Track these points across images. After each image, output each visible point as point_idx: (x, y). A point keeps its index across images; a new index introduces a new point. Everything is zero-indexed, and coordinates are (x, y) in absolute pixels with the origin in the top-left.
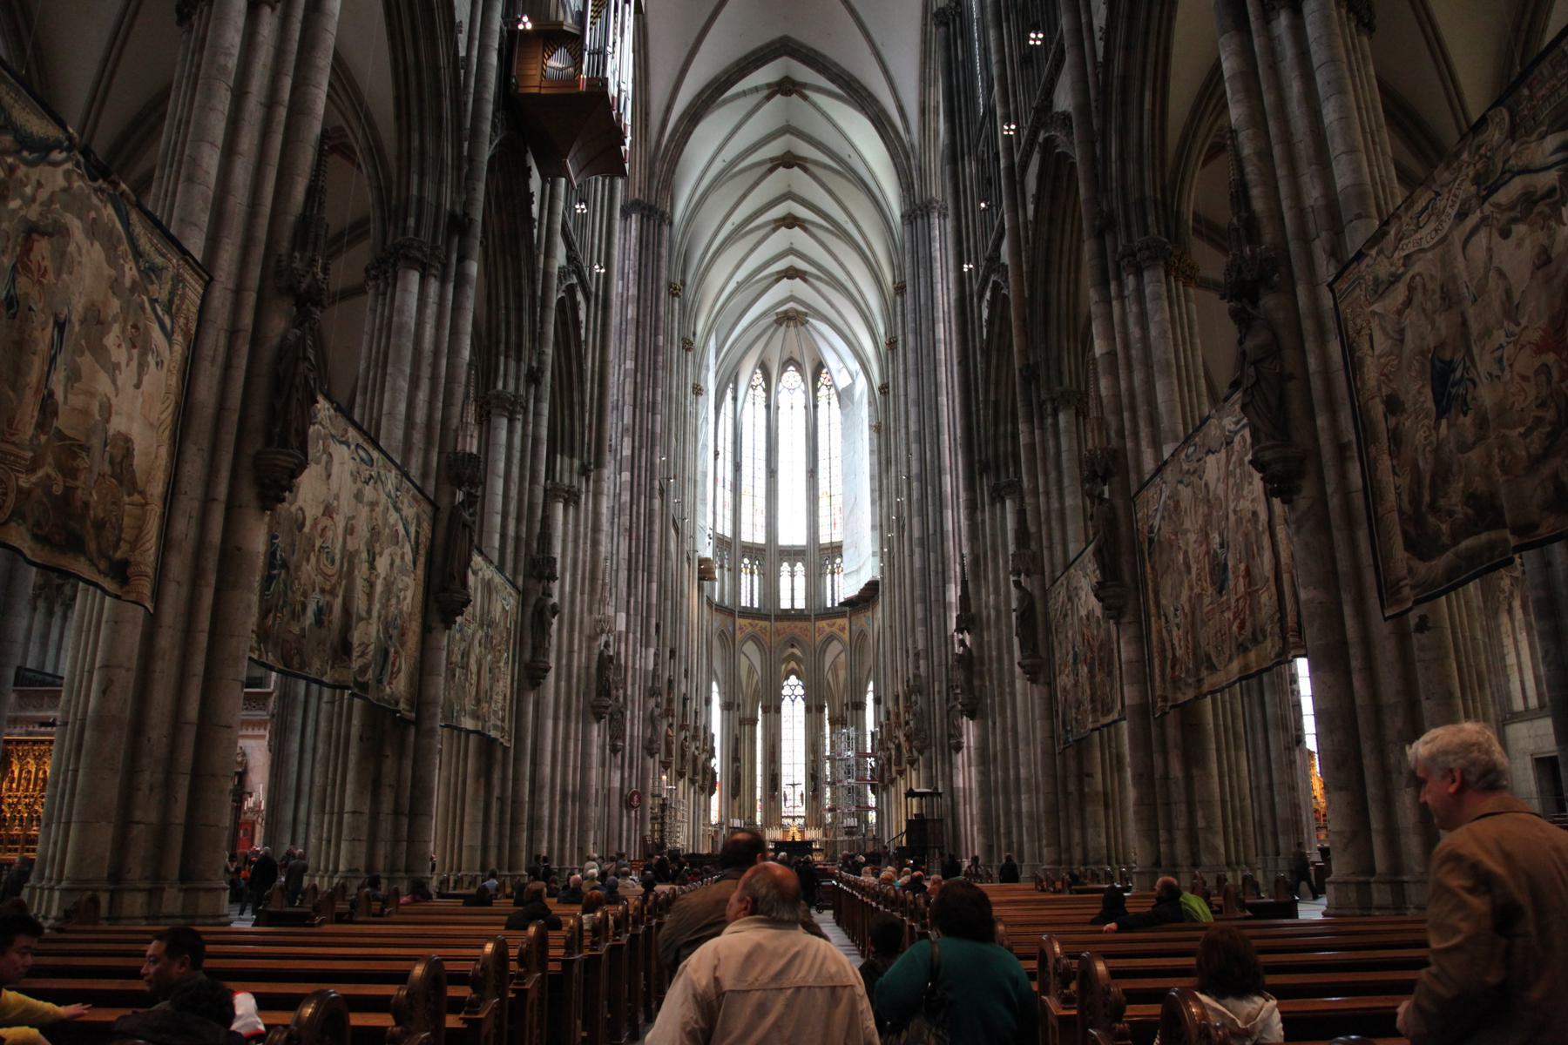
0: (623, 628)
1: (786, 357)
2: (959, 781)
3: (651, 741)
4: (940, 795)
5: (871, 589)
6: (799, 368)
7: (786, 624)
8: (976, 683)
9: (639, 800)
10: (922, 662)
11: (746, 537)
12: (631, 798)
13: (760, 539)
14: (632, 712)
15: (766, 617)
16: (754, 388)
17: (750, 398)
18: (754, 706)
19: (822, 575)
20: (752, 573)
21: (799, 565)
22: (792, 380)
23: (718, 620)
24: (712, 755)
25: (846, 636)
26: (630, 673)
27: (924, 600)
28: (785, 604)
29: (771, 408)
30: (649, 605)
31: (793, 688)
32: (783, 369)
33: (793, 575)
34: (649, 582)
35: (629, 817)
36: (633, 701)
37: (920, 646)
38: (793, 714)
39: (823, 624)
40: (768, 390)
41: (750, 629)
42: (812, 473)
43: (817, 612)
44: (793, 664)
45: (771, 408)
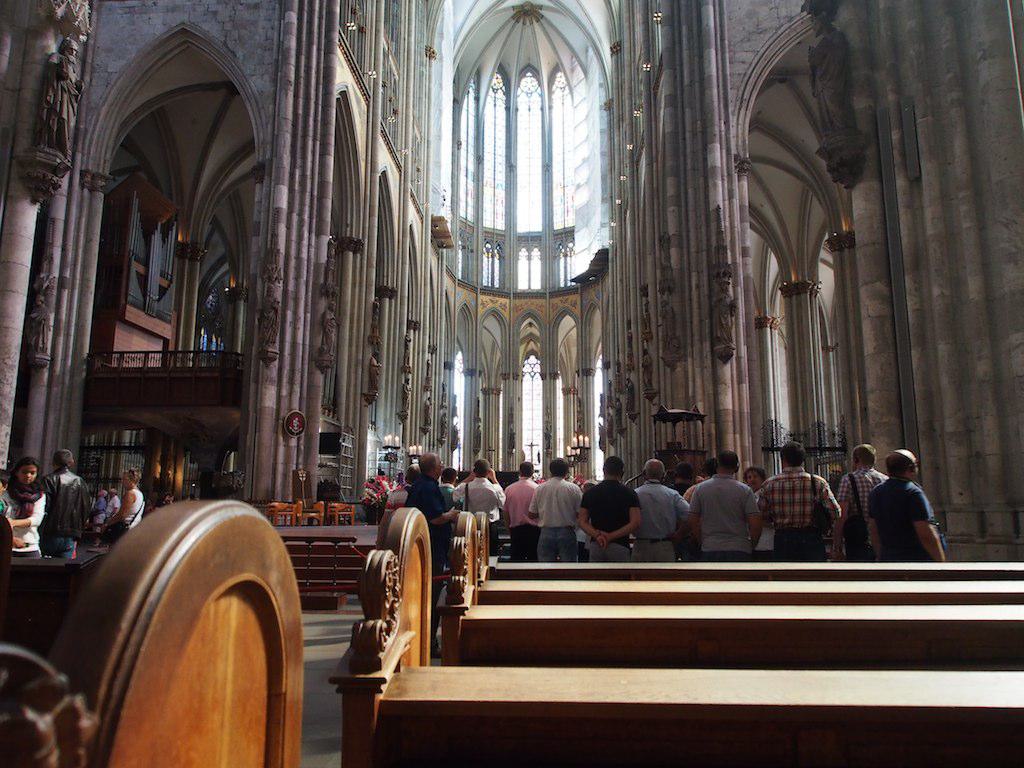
0: (284, 204)
1: (523, 64)
2: (728, 402)
3: (321, 351)
4: (701, 418)
5: (602, 257)
6: (536, 74)
7: (523, 301)
8: (860, 103)
9: (302, 424)
10: (673, 252)
11: (488, 223)
12: (289, 421)
13: (500, 225)
14: (295, 313)
15: (506, 295)
16: (495, 91)
17: (490, 100)
18: (496, 381)
19: (556, 258)
20: (493, 257)
21: (536, 250)
22: (529, 85)
23: (460, 297)
24: (454, 414)
25: (577, 311)
26: (293, 263)
27: (676, 175)
28: (522, 286)
29: (510, 110)
30: (323, 184)
31: (532, 366)
32: (522, 74)
33: (529, 258)
34: (324, 154)
35: (287, 446)
36: (296, 300)
37: (672, 230)
38: (532, 388)
39: (556, 301)
40: (507, 93)
41: (490, 305)
42: (547, 168)
43: (552, 292)
44: (532, 345)
45: (510, 110)
